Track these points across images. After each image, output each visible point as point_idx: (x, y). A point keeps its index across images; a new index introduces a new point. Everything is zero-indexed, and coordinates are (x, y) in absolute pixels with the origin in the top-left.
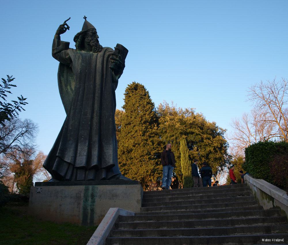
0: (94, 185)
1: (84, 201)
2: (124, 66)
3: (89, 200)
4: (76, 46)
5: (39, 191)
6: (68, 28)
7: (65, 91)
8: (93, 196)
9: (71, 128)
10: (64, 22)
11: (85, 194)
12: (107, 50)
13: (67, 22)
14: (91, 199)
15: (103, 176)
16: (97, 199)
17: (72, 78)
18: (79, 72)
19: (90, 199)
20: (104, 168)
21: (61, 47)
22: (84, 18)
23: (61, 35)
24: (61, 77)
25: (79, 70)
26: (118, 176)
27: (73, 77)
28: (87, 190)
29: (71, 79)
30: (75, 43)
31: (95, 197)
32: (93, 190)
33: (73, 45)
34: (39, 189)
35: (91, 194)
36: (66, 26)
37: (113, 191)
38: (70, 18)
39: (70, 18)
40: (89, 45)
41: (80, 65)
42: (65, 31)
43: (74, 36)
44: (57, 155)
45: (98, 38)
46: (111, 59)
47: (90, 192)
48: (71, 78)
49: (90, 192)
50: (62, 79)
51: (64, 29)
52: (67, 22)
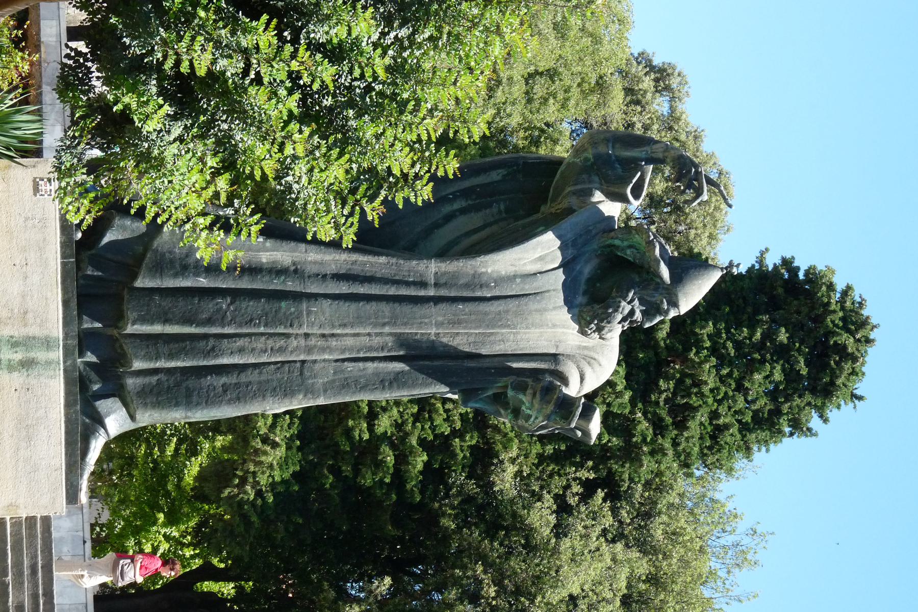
0: (65, 362)
1: (12, 337)
3: (16, 352)
5: (44, 188)
7: (444, 194)
8: (27, 364)
9: (264, 260)
11: (34, 338)
12: (592, 361)
14: (20, 360)
16: (17, 378)
17: (500, 212)
18: (483, 270)
19: (18, 356)
24: (500, 171)
25: (489, 271)
27: (504, 215)
28: (47, 343)
29: (495, 210)
31: (26, 374)
32: (49, 363)
34: (48, 187)
35: (33, 359)
41: (513, 269)
47: (41, 355)
48: (502, 207)
49: (41, 355)
50: (495, 176)
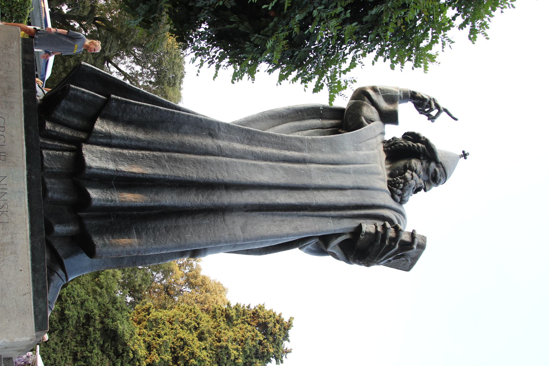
2: (368, 264)
4: (393, 139)
6: (432, 119)
10: (445, 107)
13: (444, 114)
15: (59, 229)
20: (82, 226)
21: (384, 105)
22: (463, 152)
23: (410, 105)
26: (60, 272)
30: (399, 136)
33: (393, 132)
36: (433, 113)
37: (11, 253)
38: (456, 119)
39: (456, 119)
40: (405, 169)
42: (422, 112)
43: (417, 131)
44: (113, 96)
45: (425, 190)
46: (384, 226)
51: (426, 110)
52: (444, 114)
